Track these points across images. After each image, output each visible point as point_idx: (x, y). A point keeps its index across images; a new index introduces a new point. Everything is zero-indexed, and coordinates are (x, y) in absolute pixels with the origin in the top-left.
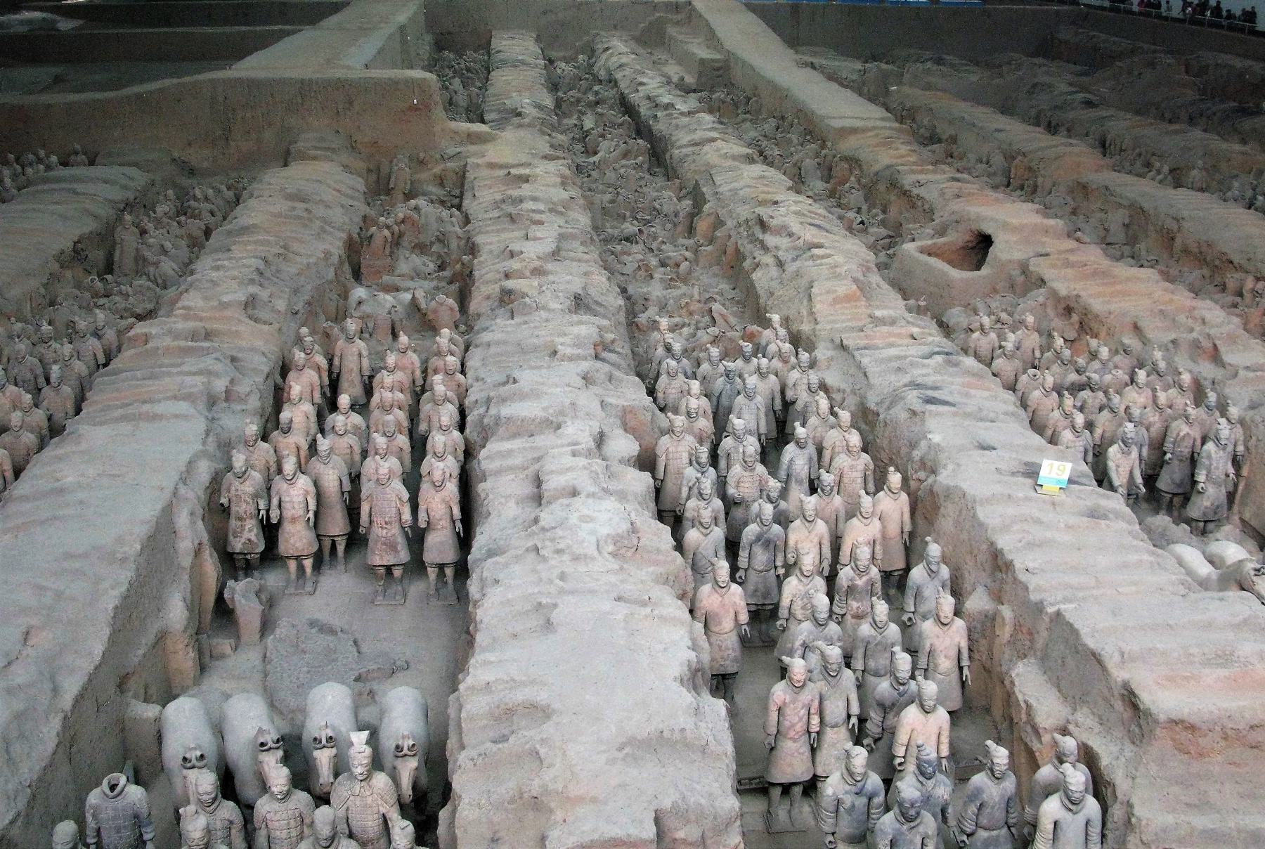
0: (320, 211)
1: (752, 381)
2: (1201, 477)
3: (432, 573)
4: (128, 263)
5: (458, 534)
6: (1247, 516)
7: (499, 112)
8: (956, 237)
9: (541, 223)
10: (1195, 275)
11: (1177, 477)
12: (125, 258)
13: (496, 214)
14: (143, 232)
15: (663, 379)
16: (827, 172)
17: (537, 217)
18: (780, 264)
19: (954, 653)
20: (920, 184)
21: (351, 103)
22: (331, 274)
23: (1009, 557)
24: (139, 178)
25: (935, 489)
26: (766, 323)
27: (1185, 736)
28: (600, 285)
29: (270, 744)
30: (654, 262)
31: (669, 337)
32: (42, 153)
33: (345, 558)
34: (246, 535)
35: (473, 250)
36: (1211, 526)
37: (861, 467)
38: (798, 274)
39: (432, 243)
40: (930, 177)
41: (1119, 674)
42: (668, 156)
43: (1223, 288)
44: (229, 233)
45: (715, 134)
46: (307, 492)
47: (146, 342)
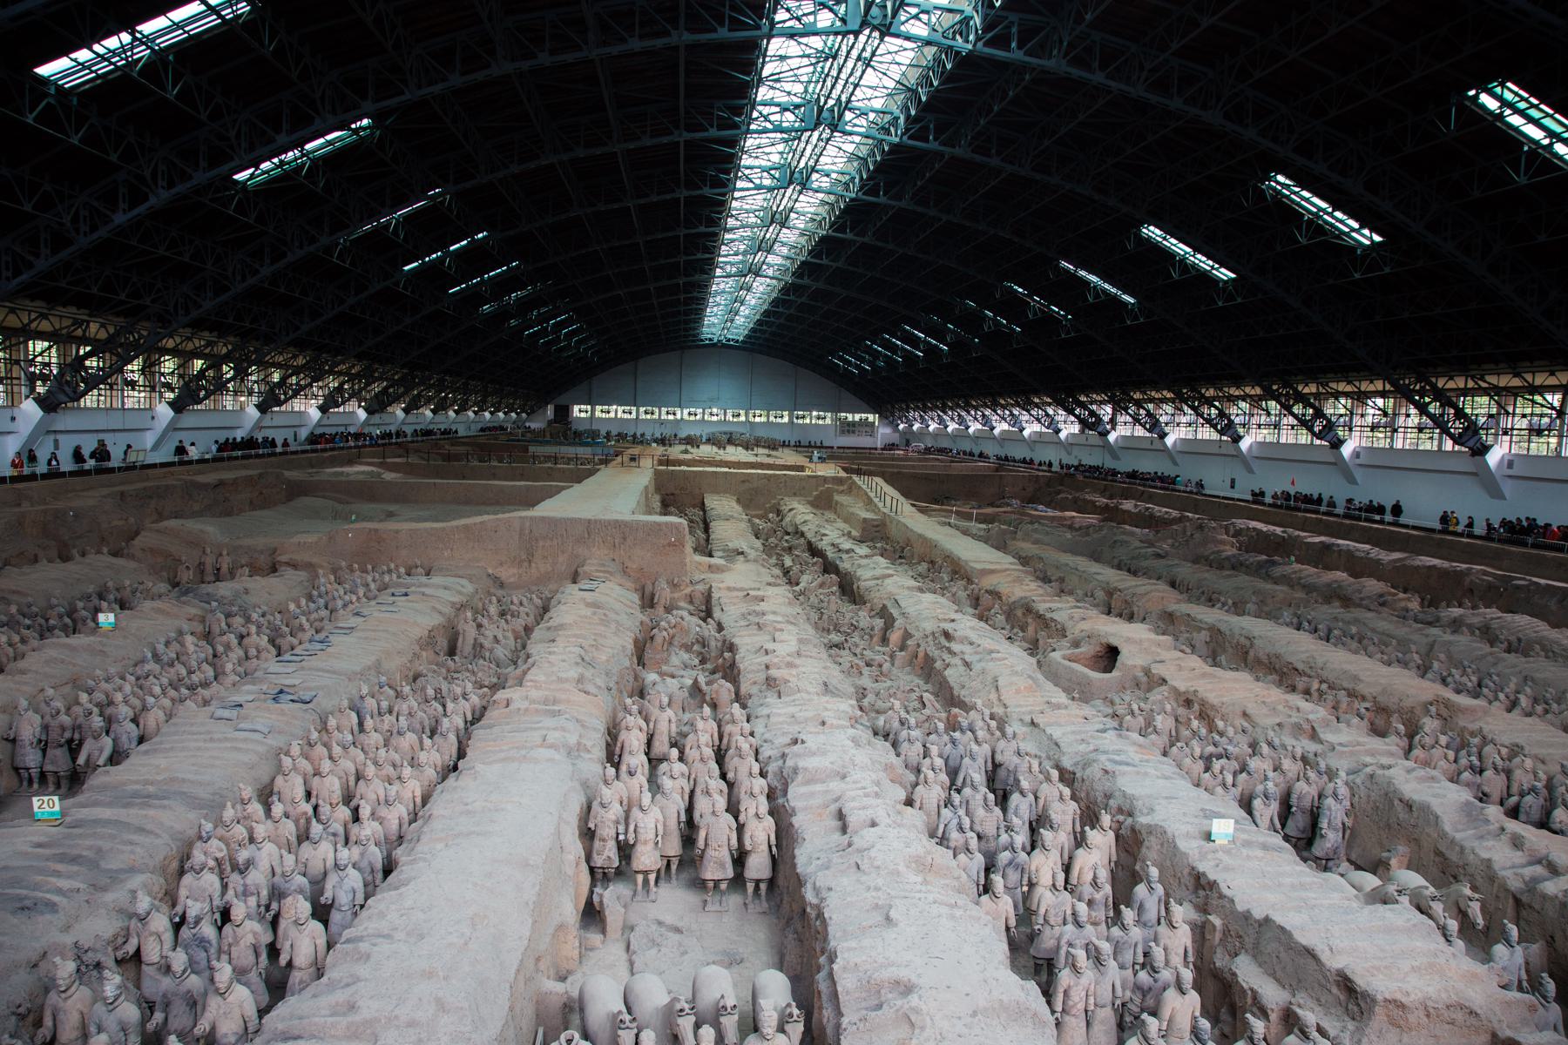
0: (612, 615)
1: (975, 747)
2: (1324, 824)
3: (750, 887)
4: (468, 649)
5: (773, 857)
6: (1353, 857)
7: (724, 551)
8: (1086, 649)
9: (782, 630)
10: (1275, 677)
11: (1301, 825)
12: (465, 645)
13: (743, 623)
14: (479, 626)
15: (904, 747)
16: (976, 601)
17: (779, 626)
18: (967, 664)
19: (1182, 952)
20: (1051, 610)
21: (625, 539)
22: (627, 663)
23: (1212, 877)
24: (469, 588)
25: (1137, 827)
26: (966, 707)
27: (1396, 1013)
28: (835, 675)
29: (687, 1011)
30: (862, 664)
31: (903, 714)
32: (392, 566)
33: (677, 874)
34: (606, 853)
35: (732, 648)
36: (1331, 864)
37: (1072, 812)
38: (983, 672)
39: (693, 644)
40: (1059, 605)
41: (1334, 962)
42: (855, 587)
43: (1293, 689)
44: (549, 628)
45: (890, 572)
46: (657, 821)
47: (507, 706)
